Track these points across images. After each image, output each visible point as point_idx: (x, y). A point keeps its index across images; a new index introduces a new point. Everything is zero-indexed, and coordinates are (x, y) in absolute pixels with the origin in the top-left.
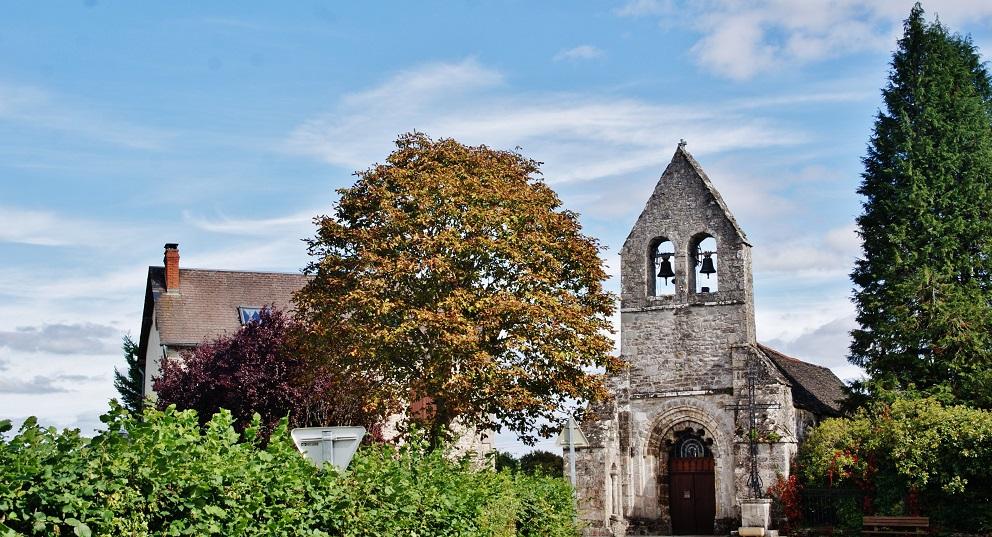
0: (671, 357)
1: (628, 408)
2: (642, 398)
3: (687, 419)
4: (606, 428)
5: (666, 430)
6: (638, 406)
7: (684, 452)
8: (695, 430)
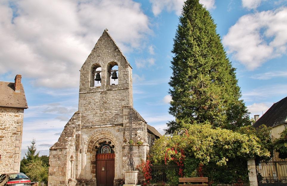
0: (98, 111)
1: (80, 132)
2: (86, 128)
3: (104, 137)
4: (69, 140)
5: (95, 142)
6: (84, 132)
7: (102, 151)
8: (107, 142)
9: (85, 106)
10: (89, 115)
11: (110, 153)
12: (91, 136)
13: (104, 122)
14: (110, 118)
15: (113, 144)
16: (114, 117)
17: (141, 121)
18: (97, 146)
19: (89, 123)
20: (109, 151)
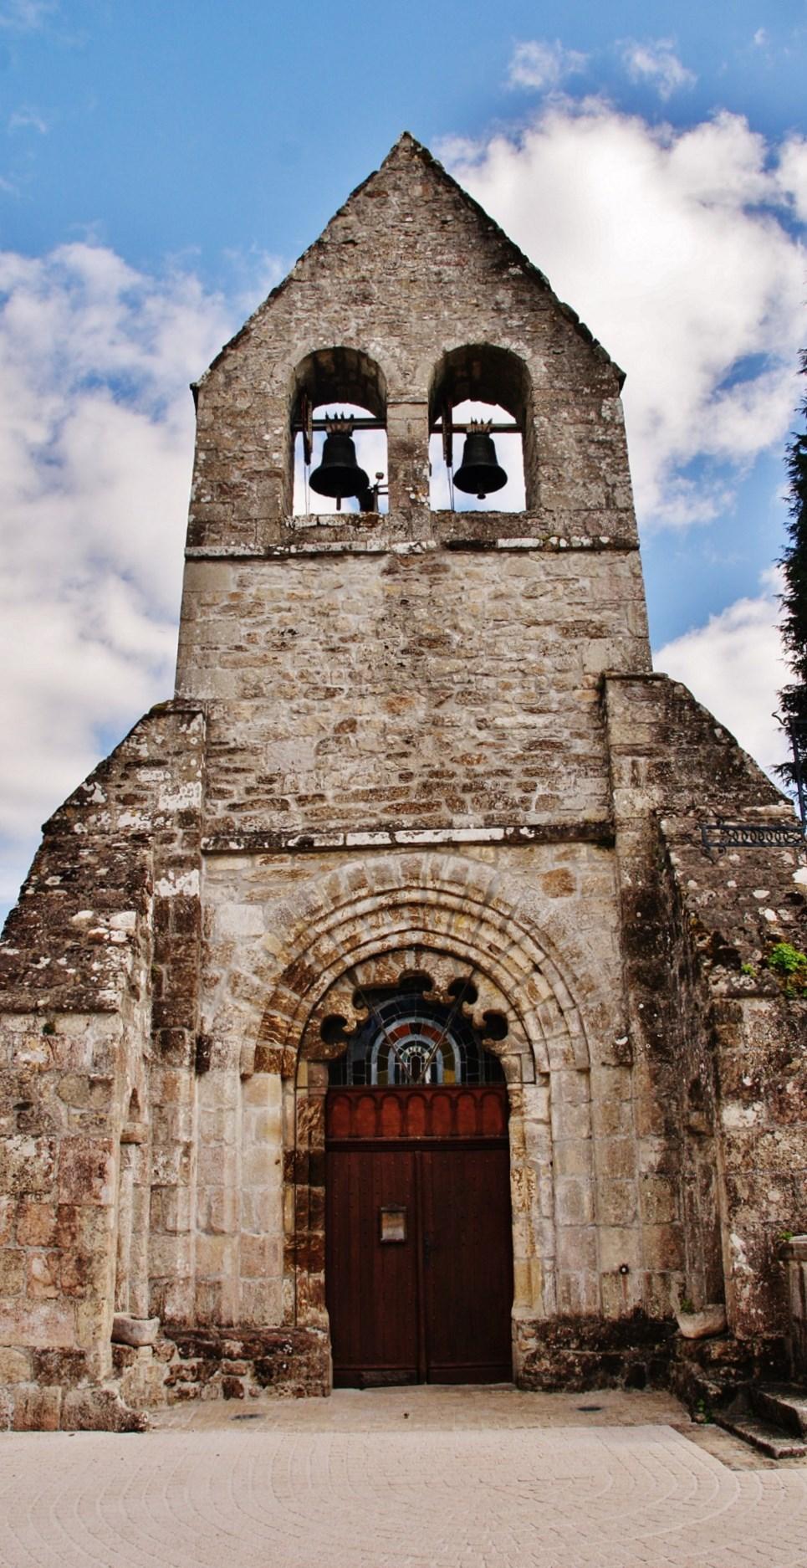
0: (371, 712)
1: (190, 883)
2: (250, 852)
3: (415, 937)
4: (119, 937)
5: (327, 978)
6: (233, 878)
7: (383, 1064)
8: (441, 983)
9: (236, 664)
10: (277, 737)
11: (452, 1088)
12: (300, 926)
13: (428, 807)
14: (480, 769)
15: (500, 1004)
16: (517, 769)
17: (775, 802)
18: (342, 1021)
19: (284, 805)
20: (449, 1064)
